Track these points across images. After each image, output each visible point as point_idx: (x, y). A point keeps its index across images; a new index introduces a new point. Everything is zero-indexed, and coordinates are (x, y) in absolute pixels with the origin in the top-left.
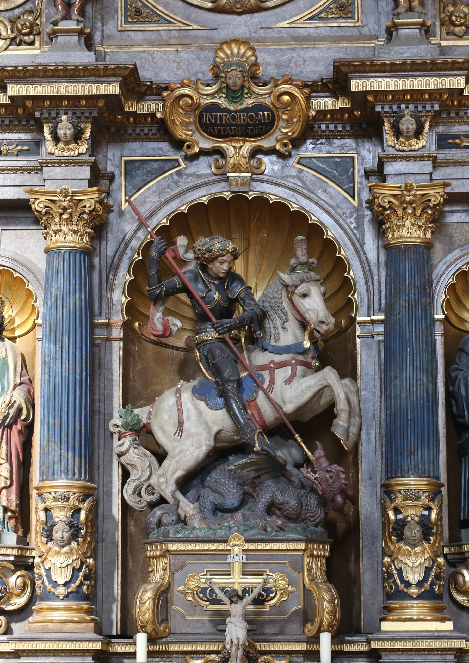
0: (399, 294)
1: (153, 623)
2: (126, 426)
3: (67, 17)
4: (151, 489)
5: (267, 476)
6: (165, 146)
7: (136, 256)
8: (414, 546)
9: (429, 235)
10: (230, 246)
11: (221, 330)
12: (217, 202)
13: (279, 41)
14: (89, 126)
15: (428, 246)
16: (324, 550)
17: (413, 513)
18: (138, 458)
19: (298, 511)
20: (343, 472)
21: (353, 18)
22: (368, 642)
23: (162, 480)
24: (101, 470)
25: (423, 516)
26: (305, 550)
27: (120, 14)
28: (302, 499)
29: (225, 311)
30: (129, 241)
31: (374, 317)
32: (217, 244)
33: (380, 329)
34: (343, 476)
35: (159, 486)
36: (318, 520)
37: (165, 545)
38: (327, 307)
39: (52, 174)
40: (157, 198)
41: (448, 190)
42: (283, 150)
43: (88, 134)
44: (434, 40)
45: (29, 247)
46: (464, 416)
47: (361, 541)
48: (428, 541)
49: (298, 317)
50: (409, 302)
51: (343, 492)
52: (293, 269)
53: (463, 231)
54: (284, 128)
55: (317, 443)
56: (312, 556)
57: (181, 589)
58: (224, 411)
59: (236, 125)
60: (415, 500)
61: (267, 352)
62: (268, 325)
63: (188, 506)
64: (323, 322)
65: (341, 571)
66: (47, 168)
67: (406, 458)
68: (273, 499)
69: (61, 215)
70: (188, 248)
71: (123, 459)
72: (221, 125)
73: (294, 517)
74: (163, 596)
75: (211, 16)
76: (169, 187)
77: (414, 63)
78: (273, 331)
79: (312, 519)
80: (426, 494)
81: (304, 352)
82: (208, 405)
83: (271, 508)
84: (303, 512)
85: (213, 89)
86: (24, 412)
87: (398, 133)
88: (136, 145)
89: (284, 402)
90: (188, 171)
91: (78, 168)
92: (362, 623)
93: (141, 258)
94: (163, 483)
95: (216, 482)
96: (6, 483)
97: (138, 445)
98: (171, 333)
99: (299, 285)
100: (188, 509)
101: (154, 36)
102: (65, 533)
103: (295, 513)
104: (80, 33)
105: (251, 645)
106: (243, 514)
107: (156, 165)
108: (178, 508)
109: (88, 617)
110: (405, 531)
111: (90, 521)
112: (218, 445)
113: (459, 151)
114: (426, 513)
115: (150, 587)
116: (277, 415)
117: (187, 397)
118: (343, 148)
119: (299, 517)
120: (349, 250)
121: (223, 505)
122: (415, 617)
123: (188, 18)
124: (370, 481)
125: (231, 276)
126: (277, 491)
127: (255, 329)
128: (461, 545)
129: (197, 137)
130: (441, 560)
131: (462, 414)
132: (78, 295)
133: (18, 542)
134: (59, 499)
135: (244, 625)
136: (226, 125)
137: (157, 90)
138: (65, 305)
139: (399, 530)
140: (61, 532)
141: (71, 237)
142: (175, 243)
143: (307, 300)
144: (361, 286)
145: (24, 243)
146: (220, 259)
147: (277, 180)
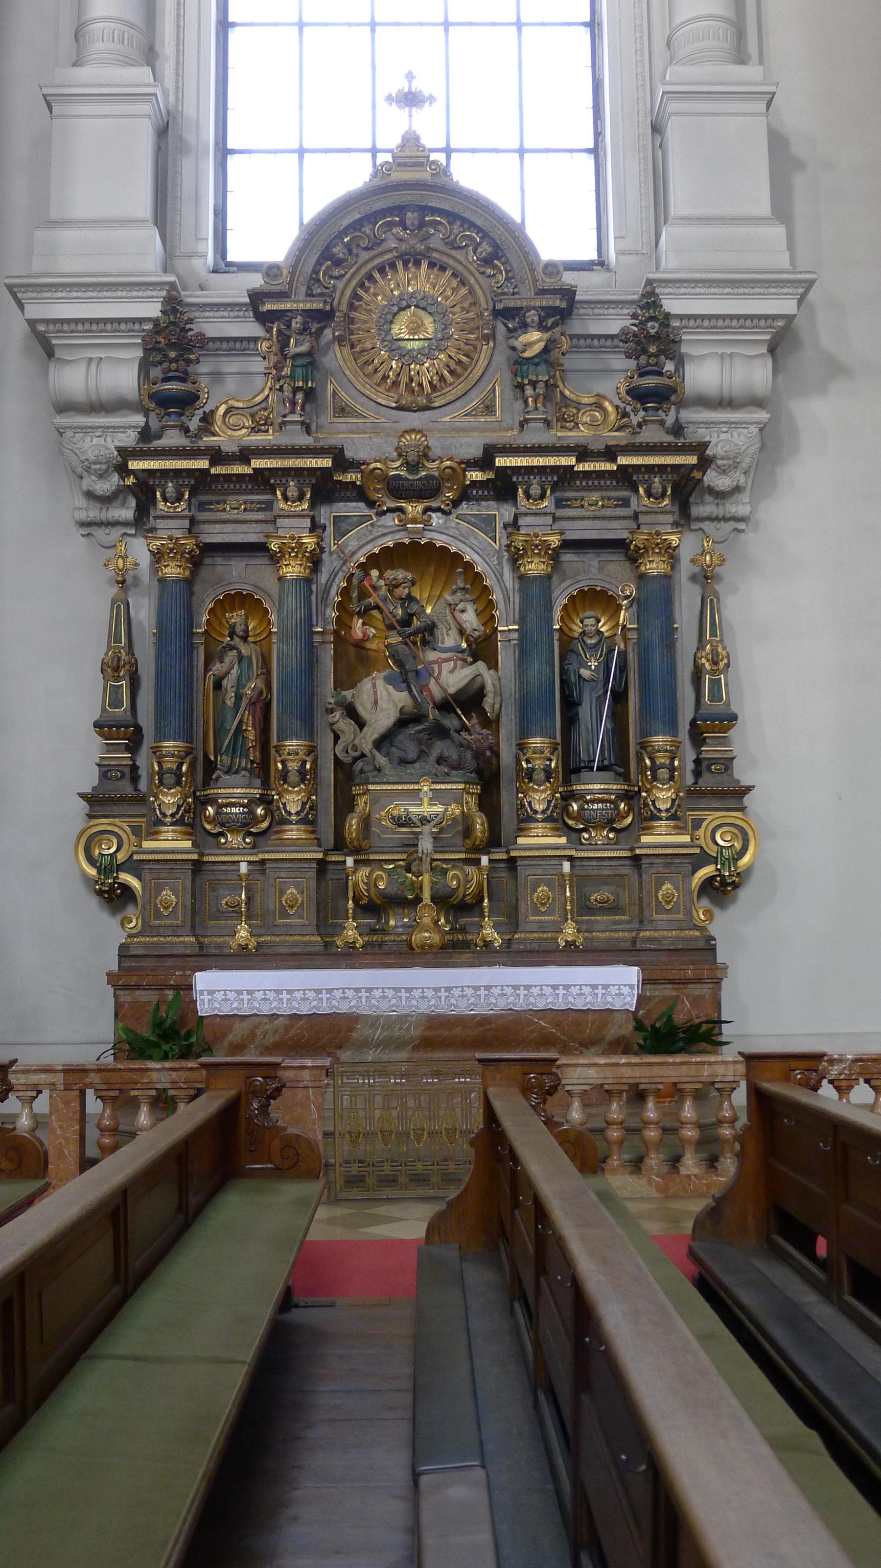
1: (358, 840)
2: (336, 703)
3: (293, 412)
6: (362, 505)
8: (540, 785)
9: (549, 569)
10: (410, 576)
12: (399, 545)
13: (440, 431)
15: (549, 577)
16: (477, 789)
17: (538, 764)
18: (345, 725)
21: (495, 415)
22: (508, 852)
23: (363, 741)
24: (319, 734)
27: (330, 411)
29: (406, 621)
30: (337, 573)
31: (510, 627)
32: (401, 574)
33: (515, 635)
34: (490, 737)
38: (479, 620)
41: (563, 537)
42: (446, 508)
44: (553, 432)
48: (550, 782)
49: (458, 626)
51: (490, 748)
52: (454, 592)
56: (469, 793)
57: (377, 816)
62: (438, 633)
65: (489, 802)
69: (290, 553)
70: (381, 577)
71: (334, 727)
74: (366, 822)
75: (394, 412)
77: (540, 447)
81: (463, 651)
82: (394, 688)
83: (440, 760)
85: (398, 464)
87: (528, 496)
88: (341, 504)
90: (378, 524)
91: (301, 520)
98: (369, 637)
101: (354, 427)
104: (303, 423)
107: (355, 519)
109: (313, 836)
112: (402, 717)
114: (548, 763)
116: (444, 696)
117: (380, 683)
118: (489, 508)
123: (378, 414)
125: (410, 598)
127: (427, 634)
128: (571, 786)
129: (385, 499)
130: (558, 795)
136: (407, 490)
137: (355, 465)
140: (293, 777)
141: (297, 569)
142: (369, 575)
143: (465, 614)
144: (501, 605)
147: (443, 530)
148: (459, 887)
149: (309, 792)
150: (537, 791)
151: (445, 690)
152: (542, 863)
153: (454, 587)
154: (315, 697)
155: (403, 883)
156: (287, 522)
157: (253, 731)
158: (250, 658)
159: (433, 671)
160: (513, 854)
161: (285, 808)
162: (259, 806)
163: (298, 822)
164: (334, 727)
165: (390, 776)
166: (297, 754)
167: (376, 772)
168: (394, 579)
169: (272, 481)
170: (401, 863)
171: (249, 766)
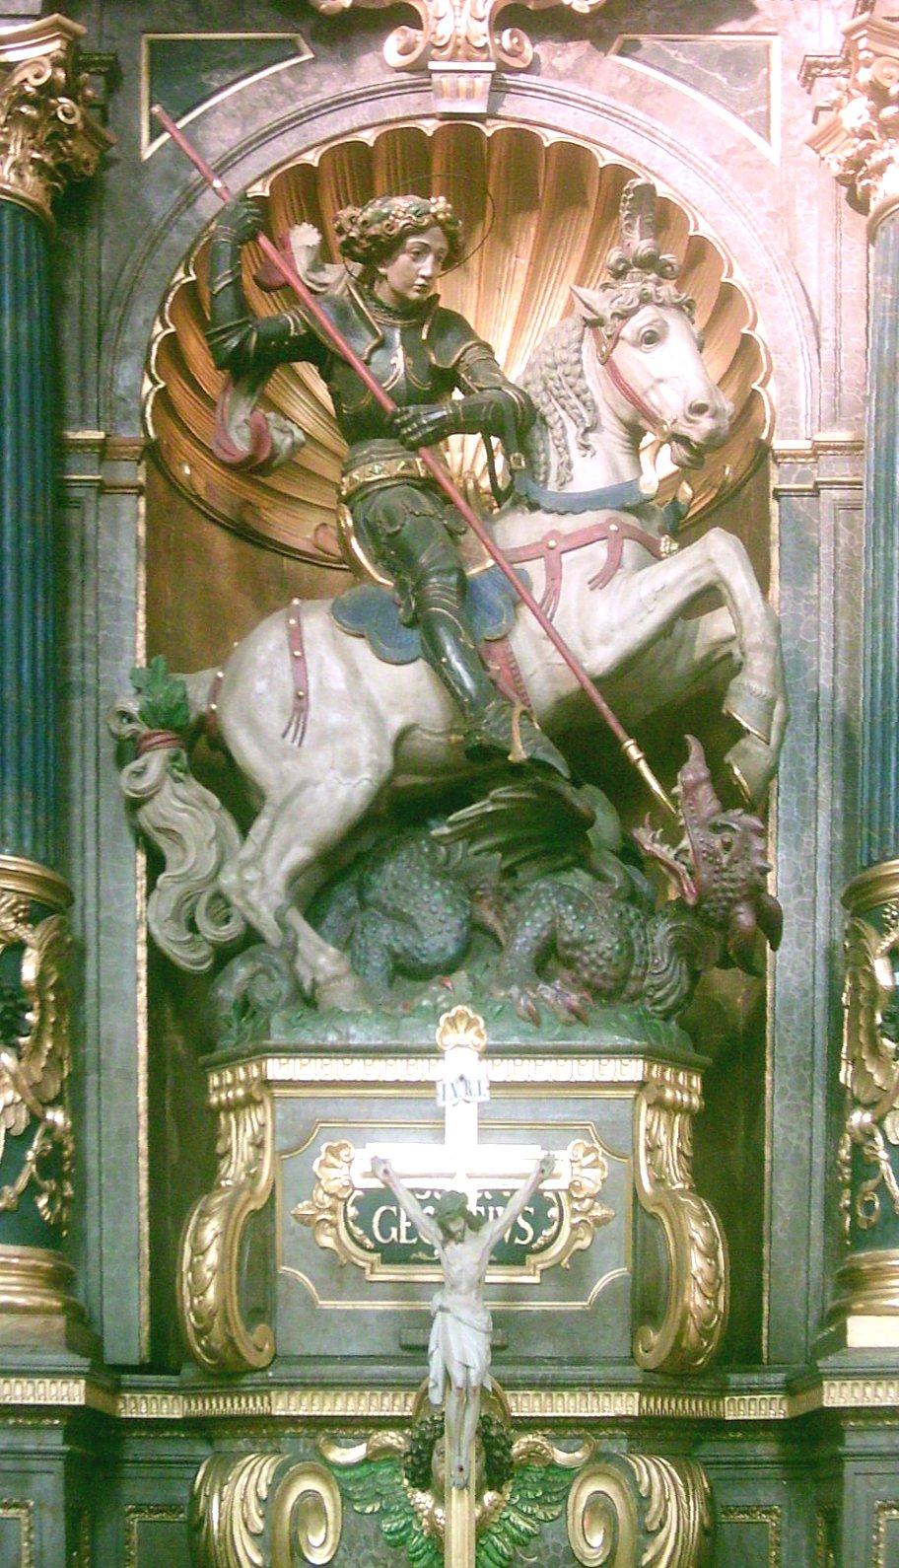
5: (534, 868)
26: (641, 1085)
35: (243, 893)
37: (259, 1067)
58: (421, 664)
61: (539, 514)
63: (321, 950)
73: (609, 985)
79: (659, 994)
83: (550, 957)
84: (633, 973)
94: (252, 883)
97: (185, 772)
100: (322, 960)
103: (612, 973)
106: (471, 977)
111: (56, 988)
112: (403, 781)
115: (219, 1199)
121: (416, 954)
135: (483, 1320)
153: (614, 255)
154: (77, 702)
160: (837, 1395)
165: (354, 1016)
170: (392, 1438)
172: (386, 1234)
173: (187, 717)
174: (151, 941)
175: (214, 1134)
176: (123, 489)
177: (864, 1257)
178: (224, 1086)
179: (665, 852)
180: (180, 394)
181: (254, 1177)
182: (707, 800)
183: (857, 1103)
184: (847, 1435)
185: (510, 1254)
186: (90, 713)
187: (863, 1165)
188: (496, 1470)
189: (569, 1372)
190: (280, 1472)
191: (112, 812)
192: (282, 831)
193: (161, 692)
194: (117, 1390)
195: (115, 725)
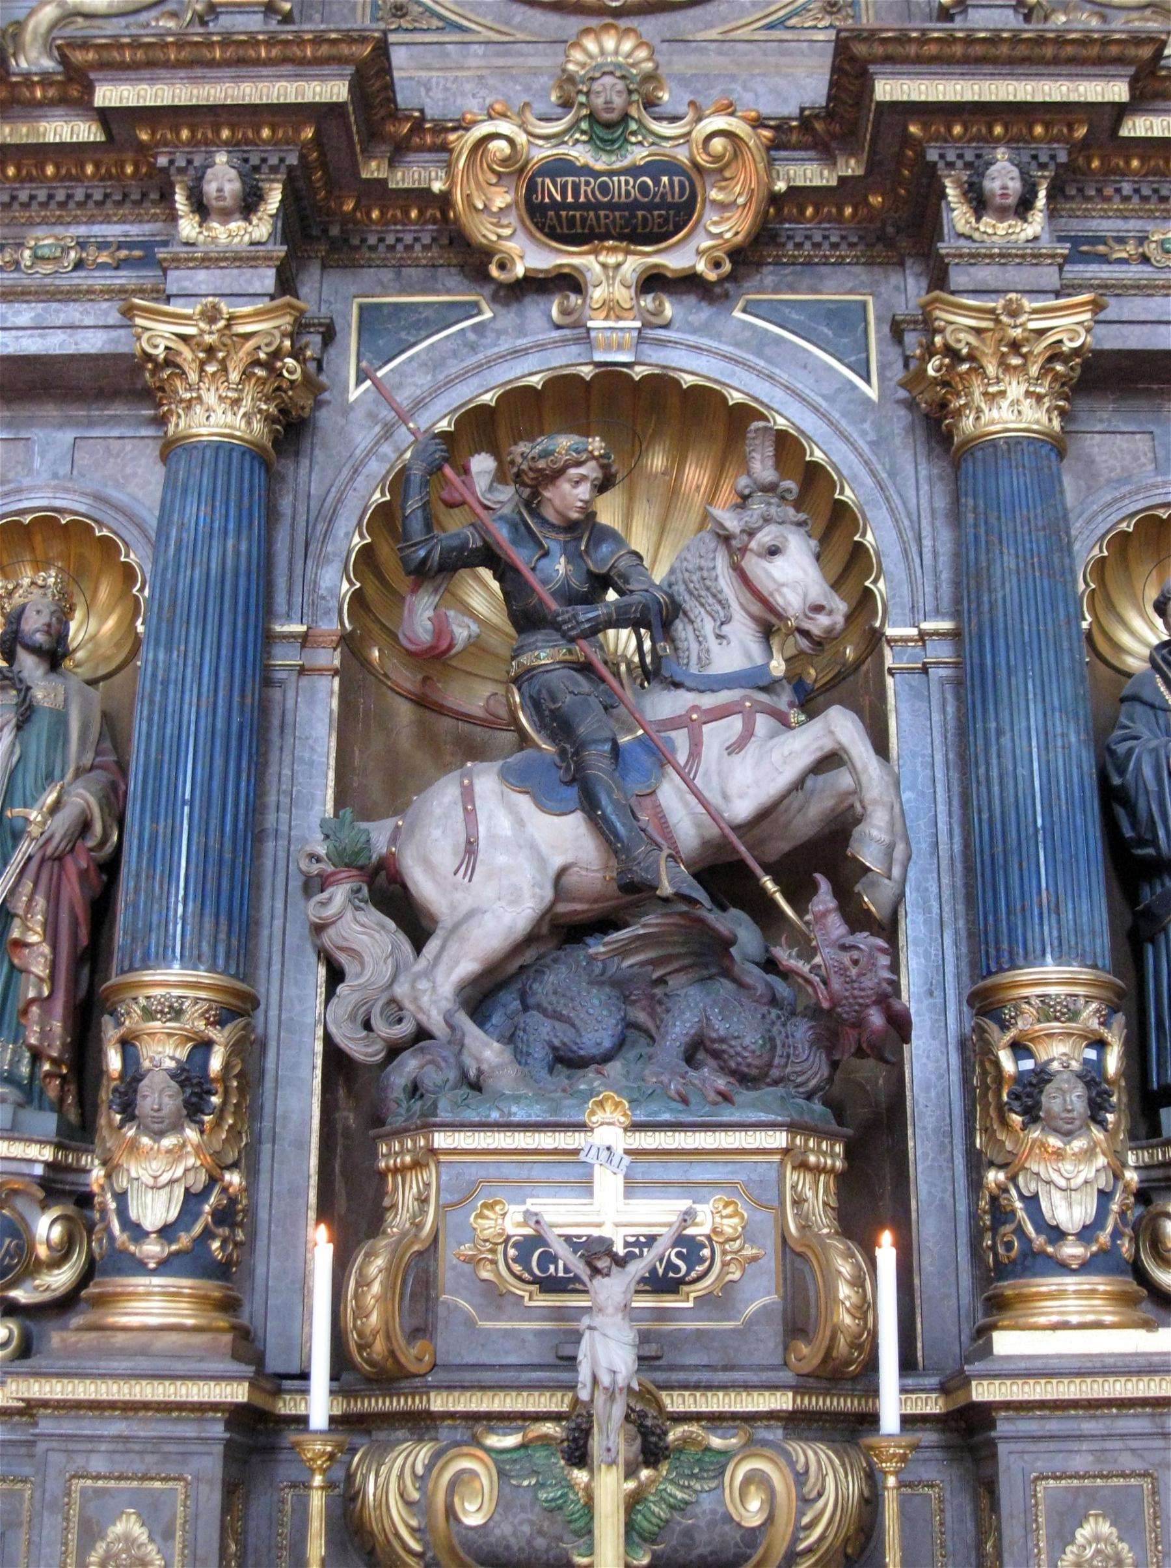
0: (1001, 543)
4: (395, 1010)
5: (682, 978)
7: (377, 495)
8: (1068, 1135)
11: (573, 628)
14: (278, 187)
15: (1058, 446)
17: (1059, 1052)
19: (766, 1058)
20: (883, 951)
25: (1086, 1061)
26: (786, 1151)
28: (775, 1030)
30: (363, 463)
32: (564, 443)
33: (941, 651)
36: (813, 1082)
37: (427, 1139)
39: (187, 284)
40: (429, 377)
42: (712, 276)
43: (274, 199)
45: (135, 474)
46: (1154, 842)
47: (911, 1144)
48: (1102, 1123)
49: (756, 608)
50: (1025, 561)
52: (744, 500)
53: (1115, 449)
54: (715, 223)
55: (818, 876)
56: (803, 1166)
57: (467, 1249)
59: (611, 206)
60: (1069, 1020)
61: (681, 692)
63: (486, 1045)
64: (818, 609)
66: (177, 273)
67: (1036, 920)
68: (701, 1028)
69: (202, 364)
72: (576, 206)
73: (754, 1072)
76: (455, 353)
78: (694, 646)
79: (799, 1080)
80: (1094, 1006)
81: (769, 687)
83: (697, 1050)
84: (776, 1061)
86: (98, 828)
87: (979, 203)
89: (725, 797)
92: (919, 1345)
93: (388, 498)
94: (425, 991)
95: (555, 993)
96: (40, 991)
99: (760, 529)
102: (166, 1100)
103: (757, 1062)
105: (646, 1395)
108: (460, 1052)
110: (1044, 1099)
111: (239, 1076)
113: (1105, 267)
115: (384, 1243)
119: (766, 1075)
120: (862, 485)
122: (1074, 1319)
123: (507, 23)
124: (931, 1000)
126: (711, 1007)
131: (1148, 836)
132: (230, 543)
133: (59, 1132)
134: (156, 1012)
136: (587, 206)
138: (198, 559)
139: (1029, 1095)
140: (160, 1095)
143: (779, 561)
144: (892, 561)
145: (124, 466)
146: (573, 471)
148: (770, 1519)
149: (216, 1155)
150: (1059, 1155)
151: (713, 814)
152: (1088, 1427)
154: (270, 845)
155: (554, 1509)
156: (202, 280)
157: (46, 949)
158: (60, 719)
159: (673, 750)
161: (122, 1212)
162: (44, 1206)
163: (165, 1266)
164: (329, 938)
165: (517, 1099)
166: (177, 1013)
167: (466, 1090)
168: (545, 454)
169: (162, 161)
170: (549, 1428)
171: (25, 1070)
172: (544, 1269)
173: (370, 858)
174: (328, 1038)
175: (381, 1193)
176: (320, 671)
177: (1008, 1287)
178: (391, 1154)
179: (803, 967)
180: (372, 593)
181: (419, 1226)
182: (836, 926)
183: (991, 1164)
184: (998, 1423)
185: (662, 1283)
186: (282, 854)
187: (1000, 1213)
188: (652, 1450)
189: (723, 1377)
190: (436, 1456)
191: (297, 934)
192: (453, 948)
193: (347, 837)
194: (278, 1392)
195: (304, 865)
